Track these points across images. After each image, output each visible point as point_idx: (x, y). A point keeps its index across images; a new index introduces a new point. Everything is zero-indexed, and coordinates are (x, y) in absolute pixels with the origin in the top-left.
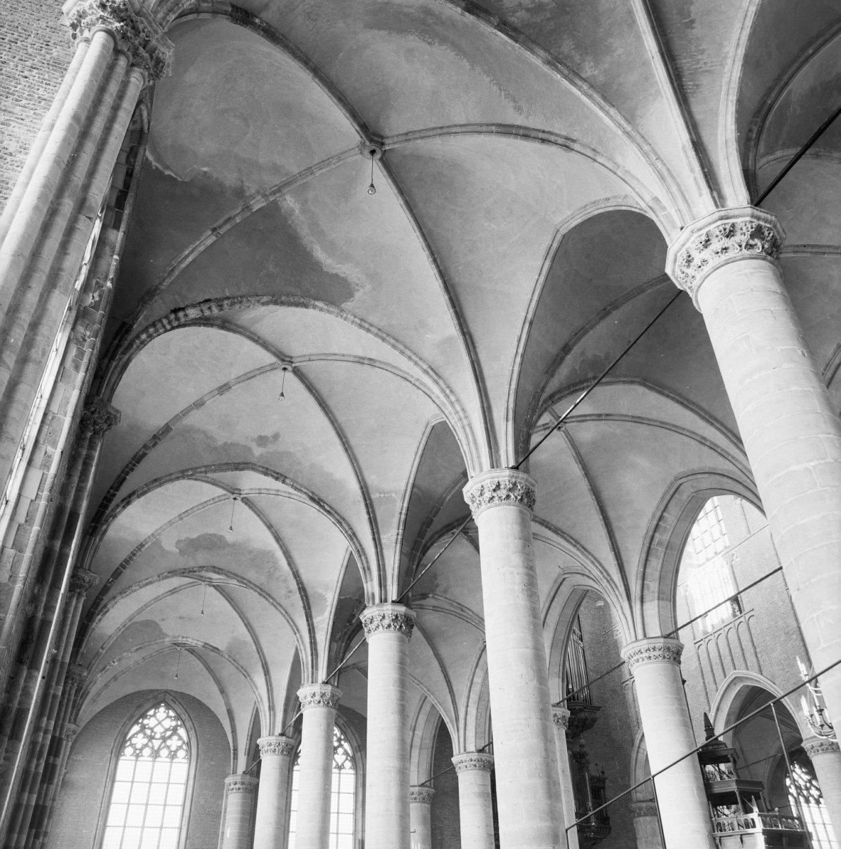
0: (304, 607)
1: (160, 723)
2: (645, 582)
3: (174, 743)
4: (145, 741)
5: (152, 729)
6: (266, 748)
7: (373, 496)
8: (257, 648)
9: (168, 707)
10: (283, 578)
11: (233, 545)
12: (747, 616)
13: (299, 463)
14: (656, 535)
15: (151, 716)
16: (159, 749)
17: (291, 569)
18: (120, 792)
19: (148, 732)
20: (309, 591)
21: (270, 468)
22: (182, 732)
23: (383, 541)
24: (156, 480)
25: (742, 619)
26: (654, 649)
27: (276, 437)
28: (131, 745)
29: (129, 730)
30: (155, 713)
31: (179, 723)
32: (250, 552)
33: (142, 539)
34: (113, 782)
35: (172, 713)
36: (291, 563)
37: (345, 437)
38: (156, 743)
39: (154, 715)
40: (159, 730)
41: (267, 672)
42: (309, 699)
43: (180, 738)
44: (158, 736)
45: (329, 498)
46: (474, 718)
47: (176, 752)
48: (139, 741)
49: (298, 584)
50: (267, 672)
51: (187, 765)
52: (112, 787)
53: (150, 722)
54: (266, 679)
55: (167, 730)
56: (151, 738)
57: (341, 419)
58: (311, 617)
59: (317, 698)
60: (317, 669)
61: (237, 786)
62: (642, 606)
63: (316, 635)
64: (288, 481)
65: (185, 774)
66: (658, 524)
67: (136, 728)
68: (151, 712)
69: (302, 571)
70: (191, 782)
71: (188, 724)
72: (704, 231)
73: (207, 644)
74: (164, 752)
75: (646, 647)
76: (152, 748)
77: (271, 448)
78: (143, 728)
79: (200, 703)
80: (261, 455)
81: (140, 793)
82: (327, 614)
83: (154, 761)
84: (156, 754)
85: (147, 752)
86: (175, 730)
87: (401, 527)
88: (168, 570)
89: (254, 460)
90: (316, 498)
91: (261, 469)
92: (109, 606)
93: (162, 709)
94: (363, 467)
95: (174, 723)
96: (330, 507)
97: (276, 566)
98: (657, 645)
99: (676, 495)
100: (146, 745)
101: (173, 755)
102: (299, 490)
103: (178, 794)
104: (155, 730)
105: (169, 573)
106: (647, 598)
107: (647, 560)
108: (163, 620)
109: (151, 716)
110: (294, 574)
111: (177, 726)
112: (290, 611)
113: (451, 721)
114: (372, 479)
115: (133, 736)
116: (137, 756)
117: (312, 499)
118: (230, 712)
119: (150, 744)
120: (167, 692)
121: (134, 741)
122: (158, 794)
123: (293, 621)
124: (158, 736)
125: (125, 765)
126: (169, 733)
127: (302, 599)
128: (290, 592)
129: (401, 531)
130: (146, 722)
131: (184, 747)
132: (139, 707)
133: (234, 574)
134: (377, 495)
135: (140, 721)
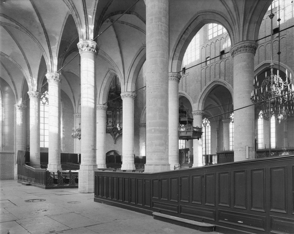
0: (47, 41)
2: (175, 53)
8: (24, 57)
10: (36, 26)
12: (186, 75)
14: (184, 35)
25: (185, 75)
26: (173, 76)
46: (102, 94)
49: (44, 30)
50: (29, 68)
54: (29, 70)
58: (50, 45)
62: (172, 61)
63: (52, 54)
66: (185, 31)
73: (2, 52)
75: (171, 75)
82: (56, 46)
87: (96, 7)
97: (34, 20)
98: (175, 75)
99: (195, 20)
106: (174, 58)
107: (178, 44)
110: (42, 25)
112: (40, 42)
127: (46, 37)
128: (40, 33)
129: (96, 9)
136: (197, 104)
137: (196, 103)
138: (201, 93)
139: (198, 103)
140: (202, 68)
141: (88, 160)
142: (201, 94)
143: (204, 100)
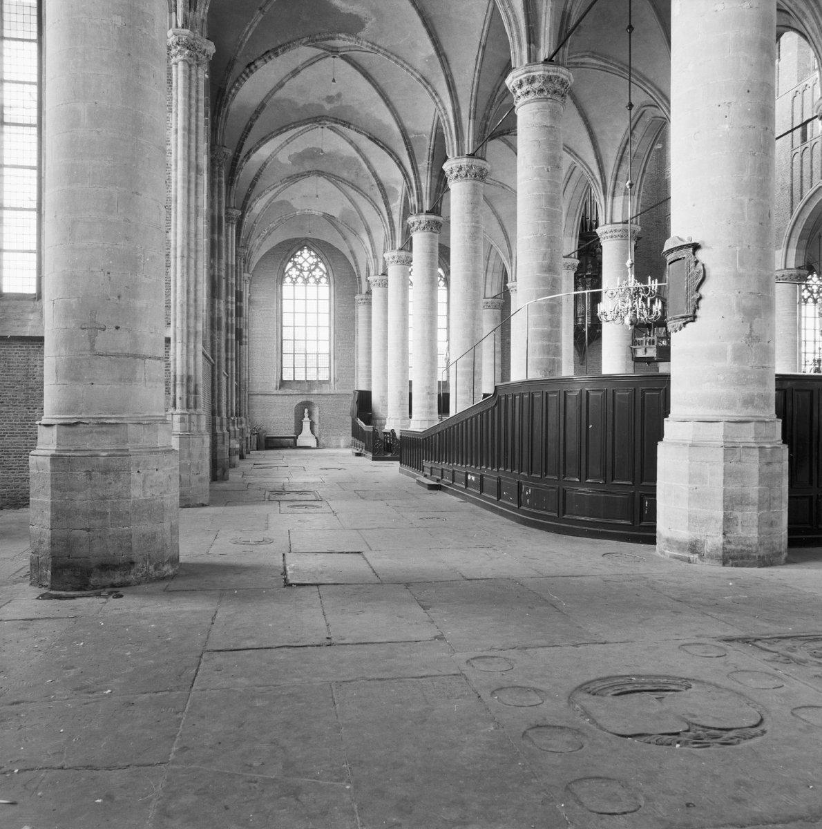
1: (306, 260)
3: (317, 273)
4: (298, 273)
5: (300, 265)
6: (374, 283)
7: (411, 137)
9: (309, 249)
11: (329, 155)
13: (358, 113)
15: (299, 256)
16: (308, 278)
17: (371, 171)
18: (287, 306)
19: (299, 267)
20: (386, 186)
21: (339, 118)
22: (321, 265)
23: (420, 169)
24: (263, 139)
27: (339, 95)
28: (289, 276)
29: (286, 266)
30: (301, 254)
31: (319, 260)
32: (342, 158)
33: (264, 159)
34: (282, 300)
35: (313, 253)
36: (370, 167)
37: (386, 95)
38: (306, 274)
39: (301, 255)
40: (306, 265)
41: (369, 233)
42: (391, 260)
43: (321, 270)
44: (306, 269)
45: (383, 137)
47: (319, 279)
48: (294, 273)
50: (369, 233)
51: (328, 288)
52: (282, 303)
53: (299, 260)
55: (311, 265)
56: (301, 271)
57: (381, 83)
59: (396, 259)
60: (395, 240)
61: (363, 301)
64: (352, 126)
65: (328, 293)
67: (290, 265)
68: (299, 253)
69: (379, 172)
70: (332, 299)
71: (325, 261)
72: (519, 79)
74: (312, 280)
76: (303, 277)
77: (336, 104)
78: (295, 264)
79: (331, 246)
80: (331, 109)
81: (300, 306)
82: (399, 201)
83: (306, 286)
84: (306, 281)
85: (300, 280)
86: (316, 265)
88: (286, 176)
89: (327, 114)
90: (373, 137)
91: (332, 119)
92: (252, 206)
93: (306, 251)
94: (402, 115)
95: (315, 260)
96: (383, 144)
97: (360, 169)
99: (642, 118)
100: (299, 276)
101: (318, 282)
102: (361, 133)
103: (325, 306)
104: (303, 265)
105: (288, 178)
106: (617, 194)
107: (619, 165)
108: (292, 199)
109: (299, 256)
111: (318, 261)
113: (507, 259)
114: (408, 124)
115: (289, 270)
116: (294, 283)
117: (370, 138)
118: (352, 252)
119: (301, 275)
120: (307, 239)
121: (290, 273)
122: (312, 306)
123: (376, 206)
124: (306, 269)
125: (287, 289)
126: (313, 267)
128: (373, 185)
130: (296, 260)
131: (325, 275)
132: (289, 251)
133: (333, 175)
134: (414, 136)
135: (292, 259)
136: (781, 250)
137: (780, 248)
138: (791, 222)
139: (785, 249)
140: (794, 152)
141: (421, 412)
142: (792, 224)
143: (801, 238)
